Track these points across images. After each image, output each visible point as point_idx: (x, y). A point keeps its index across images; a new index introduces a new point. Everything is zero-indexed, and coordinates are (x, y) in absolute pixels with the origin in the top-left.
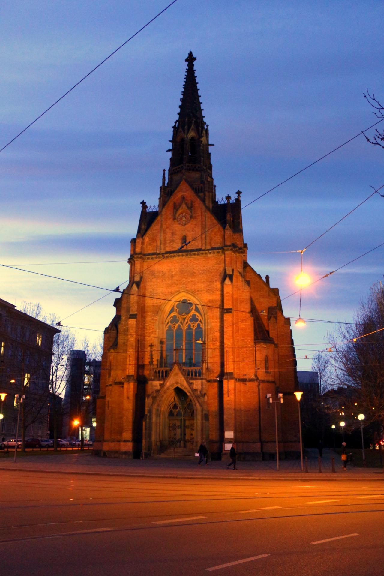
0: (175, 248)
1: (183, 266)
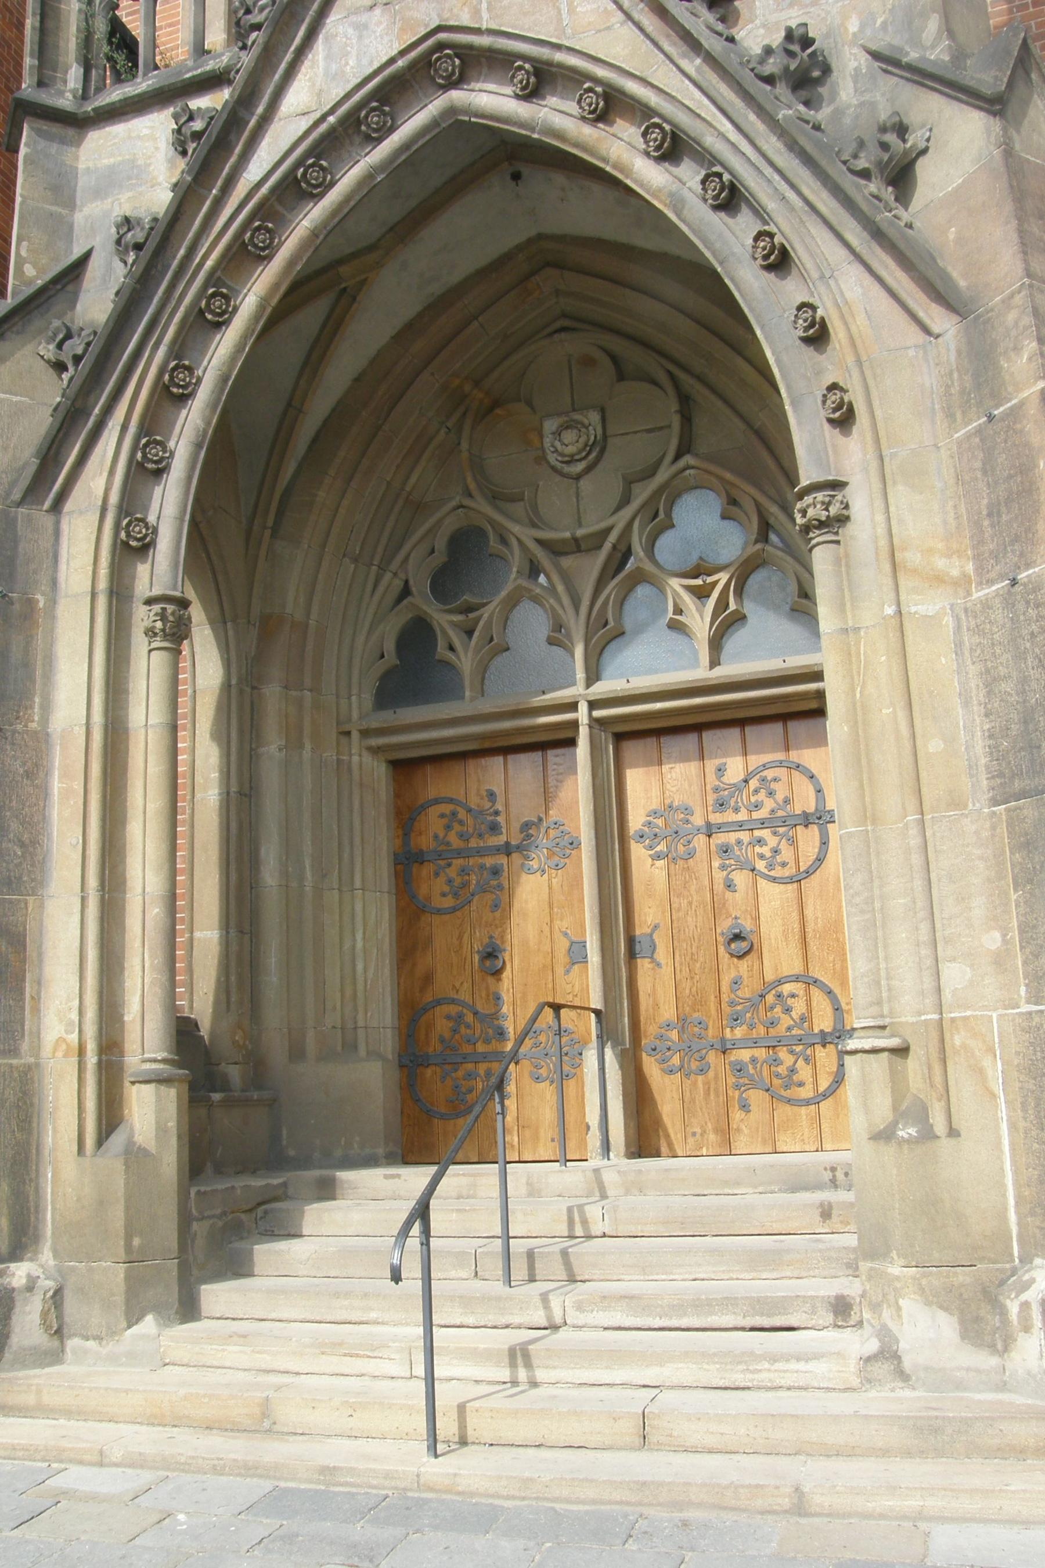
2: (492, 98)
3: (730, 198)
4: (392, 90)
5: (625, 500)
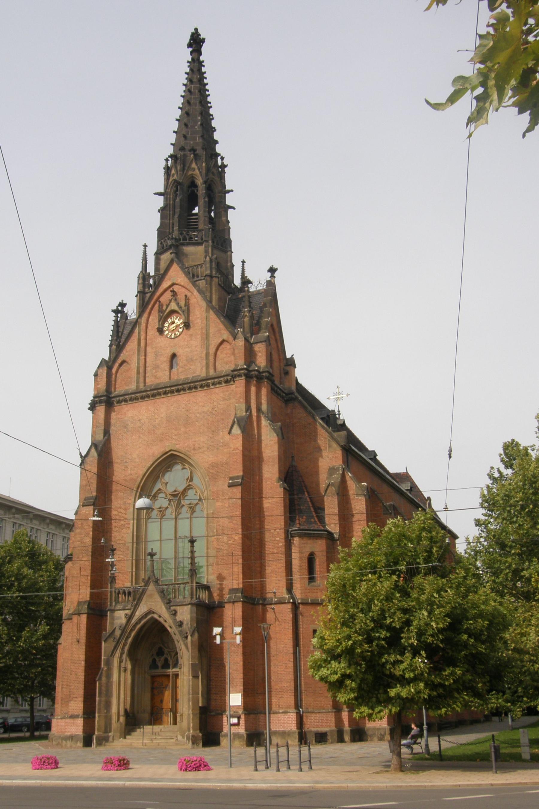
2: (156, 616)
3: (175, 634)
4: (146, 615)
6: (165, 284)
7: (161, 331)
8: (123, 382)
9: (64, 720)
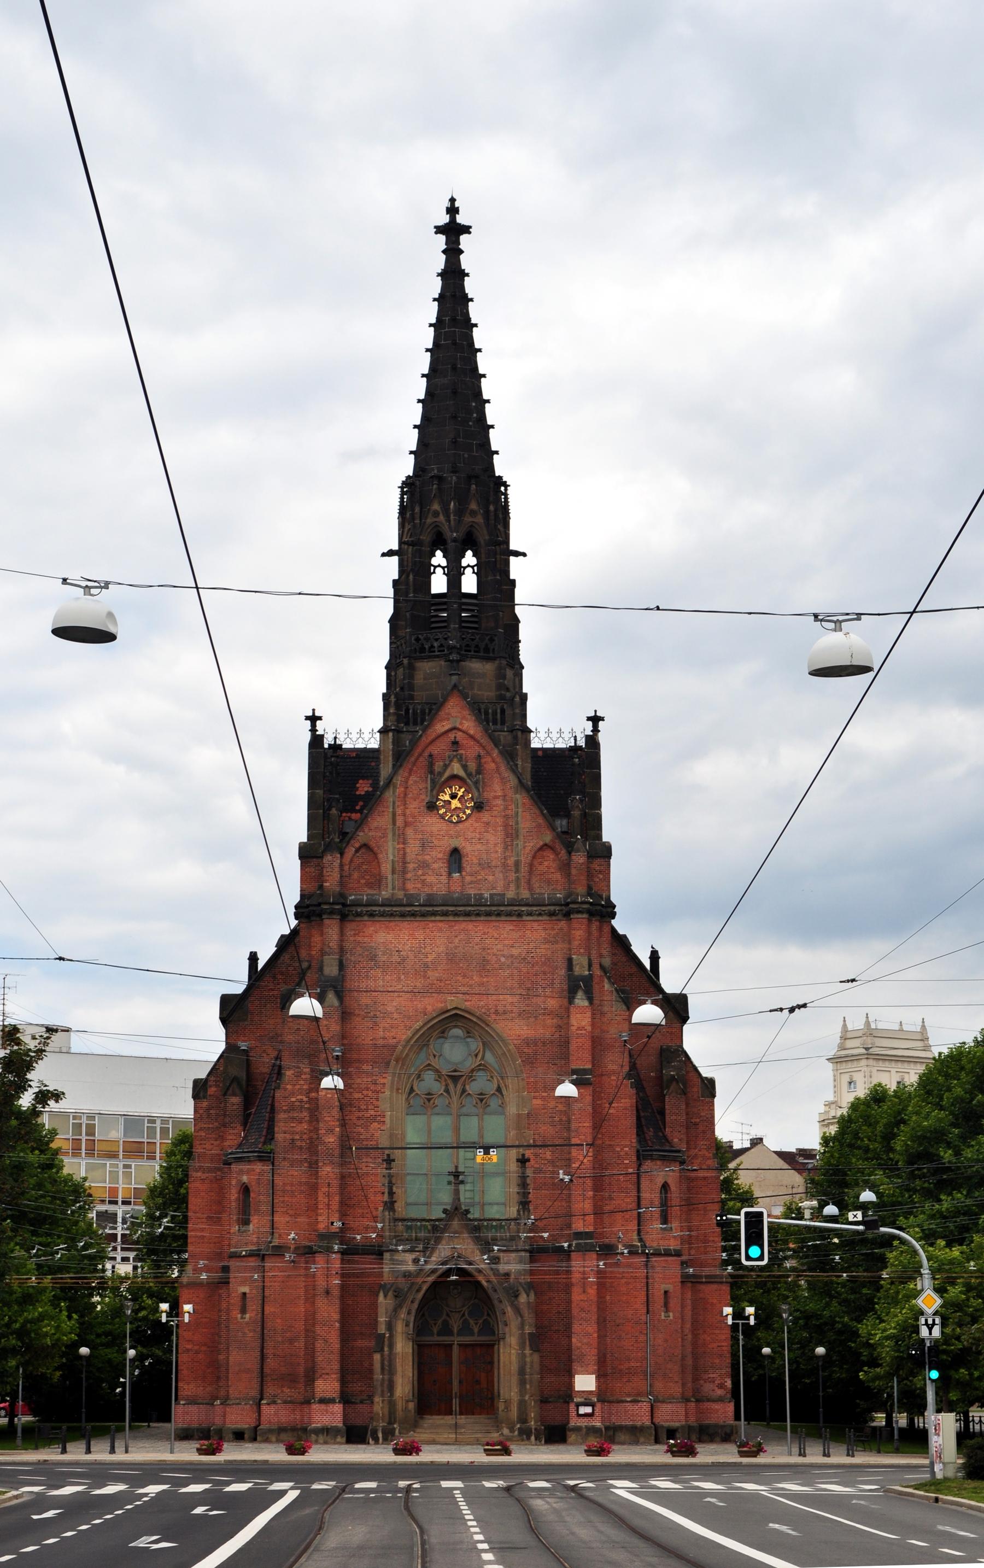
0: (431, 885)
1: (457, 941)
3: (495, 1291)
5: (463, 1306)
6: (440, 727)
7: (432, 806)
8: (363, 881)
9: (273, 1406)
